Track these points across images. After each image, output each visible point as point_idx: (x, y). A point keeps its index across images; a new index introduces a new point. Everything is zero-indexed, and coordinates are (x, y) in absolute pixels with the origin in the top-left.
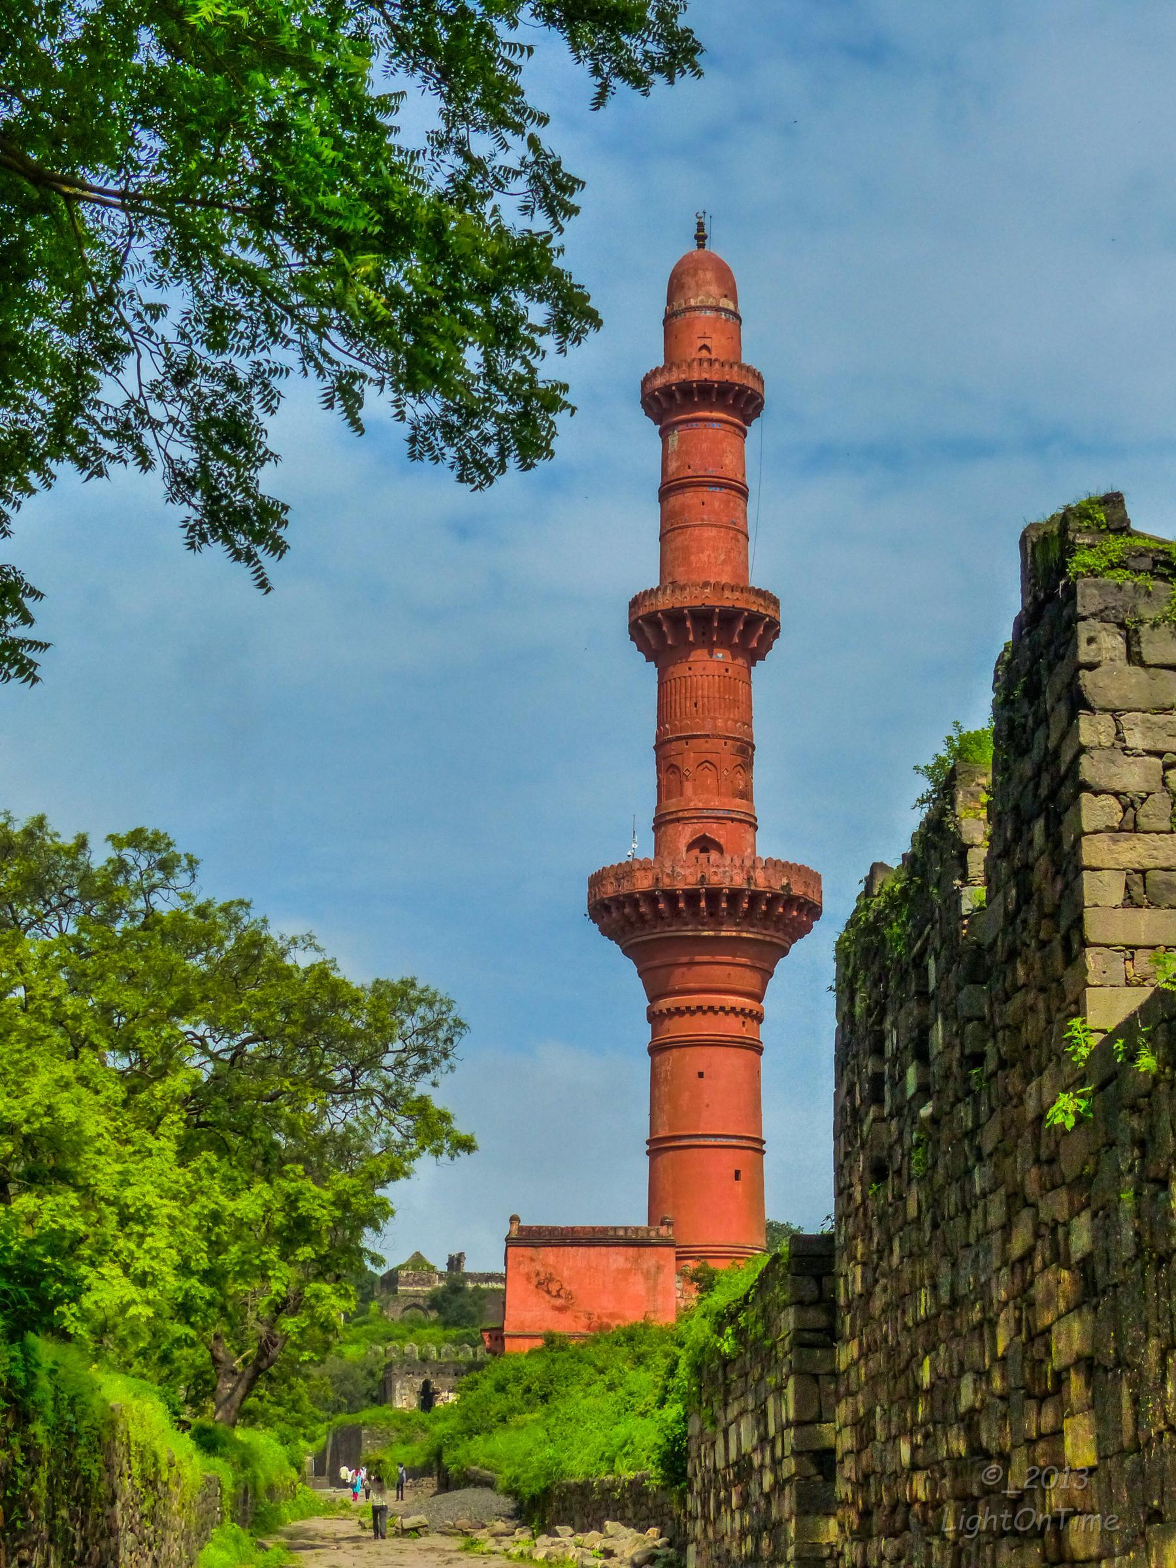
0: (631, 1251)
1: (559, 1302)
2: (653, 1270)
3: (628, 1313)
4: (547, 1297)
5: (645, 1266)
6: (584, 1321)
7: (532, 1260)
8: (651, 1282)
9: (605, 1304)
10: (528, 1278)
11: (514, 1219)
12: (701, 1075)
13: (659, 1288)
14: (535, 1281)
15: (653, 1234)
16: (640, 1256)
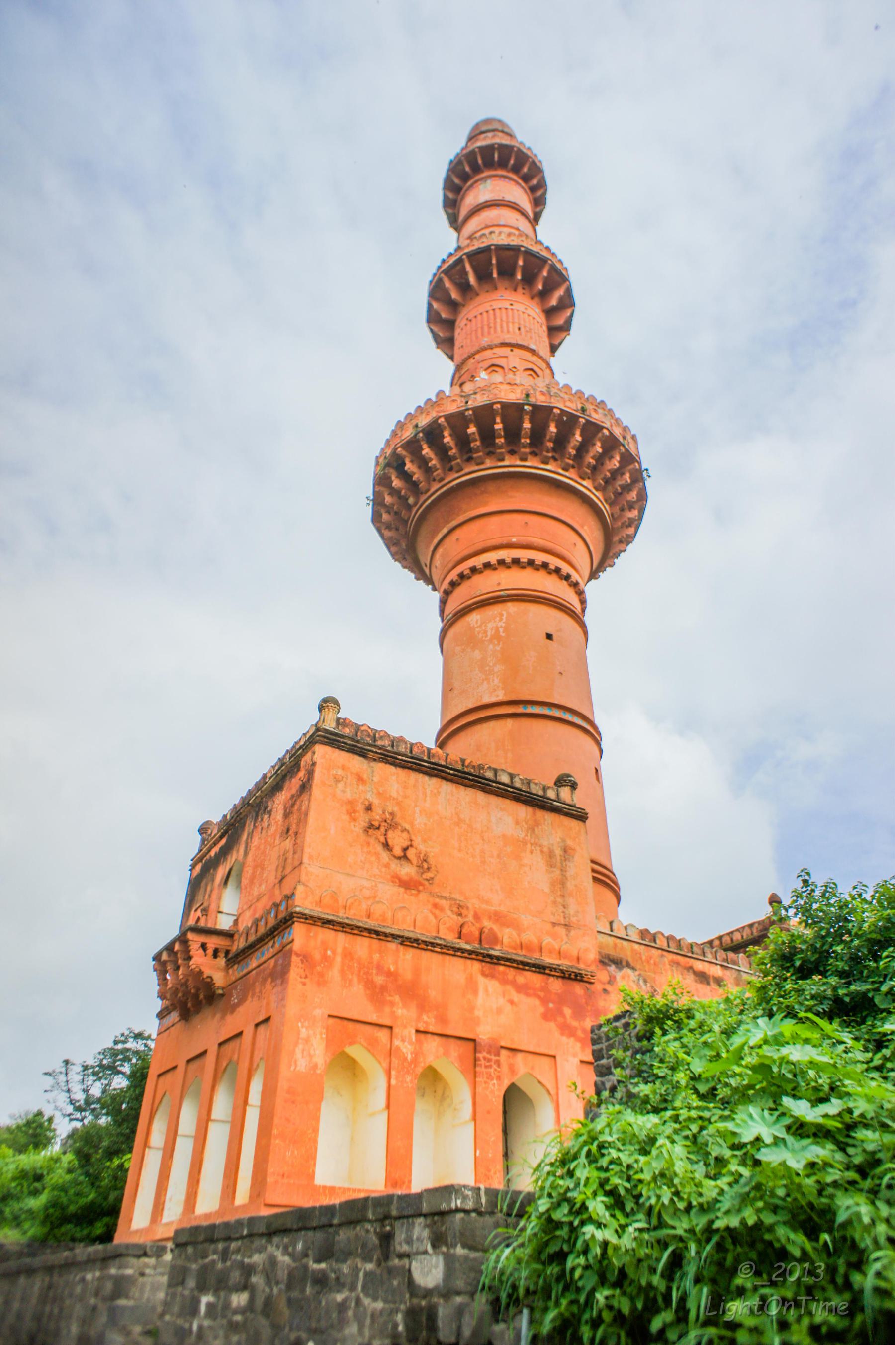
0: (523, 812)
1: (407, 870)
2: (558, 852)
3: (526, 920)
4: (385, 856)
5: (545, 843)
6: (450, 919)
7: (360, 779)
8: (558, 872)
9: (486, 894)
10: (351, 813)
11: (327, 703)
12: (549, 637)
13: (570, 885)
14: (363, 819)
15: (551, 794)
16: (537, 824)
